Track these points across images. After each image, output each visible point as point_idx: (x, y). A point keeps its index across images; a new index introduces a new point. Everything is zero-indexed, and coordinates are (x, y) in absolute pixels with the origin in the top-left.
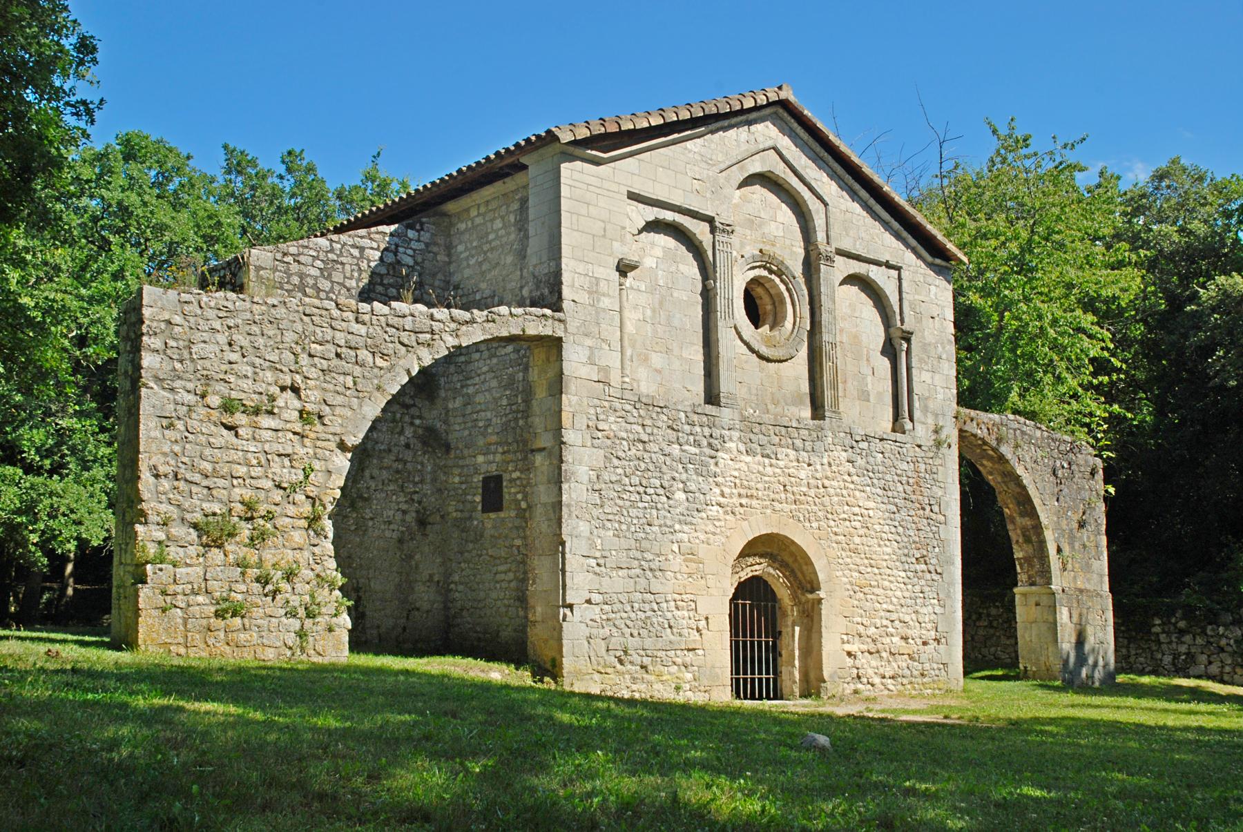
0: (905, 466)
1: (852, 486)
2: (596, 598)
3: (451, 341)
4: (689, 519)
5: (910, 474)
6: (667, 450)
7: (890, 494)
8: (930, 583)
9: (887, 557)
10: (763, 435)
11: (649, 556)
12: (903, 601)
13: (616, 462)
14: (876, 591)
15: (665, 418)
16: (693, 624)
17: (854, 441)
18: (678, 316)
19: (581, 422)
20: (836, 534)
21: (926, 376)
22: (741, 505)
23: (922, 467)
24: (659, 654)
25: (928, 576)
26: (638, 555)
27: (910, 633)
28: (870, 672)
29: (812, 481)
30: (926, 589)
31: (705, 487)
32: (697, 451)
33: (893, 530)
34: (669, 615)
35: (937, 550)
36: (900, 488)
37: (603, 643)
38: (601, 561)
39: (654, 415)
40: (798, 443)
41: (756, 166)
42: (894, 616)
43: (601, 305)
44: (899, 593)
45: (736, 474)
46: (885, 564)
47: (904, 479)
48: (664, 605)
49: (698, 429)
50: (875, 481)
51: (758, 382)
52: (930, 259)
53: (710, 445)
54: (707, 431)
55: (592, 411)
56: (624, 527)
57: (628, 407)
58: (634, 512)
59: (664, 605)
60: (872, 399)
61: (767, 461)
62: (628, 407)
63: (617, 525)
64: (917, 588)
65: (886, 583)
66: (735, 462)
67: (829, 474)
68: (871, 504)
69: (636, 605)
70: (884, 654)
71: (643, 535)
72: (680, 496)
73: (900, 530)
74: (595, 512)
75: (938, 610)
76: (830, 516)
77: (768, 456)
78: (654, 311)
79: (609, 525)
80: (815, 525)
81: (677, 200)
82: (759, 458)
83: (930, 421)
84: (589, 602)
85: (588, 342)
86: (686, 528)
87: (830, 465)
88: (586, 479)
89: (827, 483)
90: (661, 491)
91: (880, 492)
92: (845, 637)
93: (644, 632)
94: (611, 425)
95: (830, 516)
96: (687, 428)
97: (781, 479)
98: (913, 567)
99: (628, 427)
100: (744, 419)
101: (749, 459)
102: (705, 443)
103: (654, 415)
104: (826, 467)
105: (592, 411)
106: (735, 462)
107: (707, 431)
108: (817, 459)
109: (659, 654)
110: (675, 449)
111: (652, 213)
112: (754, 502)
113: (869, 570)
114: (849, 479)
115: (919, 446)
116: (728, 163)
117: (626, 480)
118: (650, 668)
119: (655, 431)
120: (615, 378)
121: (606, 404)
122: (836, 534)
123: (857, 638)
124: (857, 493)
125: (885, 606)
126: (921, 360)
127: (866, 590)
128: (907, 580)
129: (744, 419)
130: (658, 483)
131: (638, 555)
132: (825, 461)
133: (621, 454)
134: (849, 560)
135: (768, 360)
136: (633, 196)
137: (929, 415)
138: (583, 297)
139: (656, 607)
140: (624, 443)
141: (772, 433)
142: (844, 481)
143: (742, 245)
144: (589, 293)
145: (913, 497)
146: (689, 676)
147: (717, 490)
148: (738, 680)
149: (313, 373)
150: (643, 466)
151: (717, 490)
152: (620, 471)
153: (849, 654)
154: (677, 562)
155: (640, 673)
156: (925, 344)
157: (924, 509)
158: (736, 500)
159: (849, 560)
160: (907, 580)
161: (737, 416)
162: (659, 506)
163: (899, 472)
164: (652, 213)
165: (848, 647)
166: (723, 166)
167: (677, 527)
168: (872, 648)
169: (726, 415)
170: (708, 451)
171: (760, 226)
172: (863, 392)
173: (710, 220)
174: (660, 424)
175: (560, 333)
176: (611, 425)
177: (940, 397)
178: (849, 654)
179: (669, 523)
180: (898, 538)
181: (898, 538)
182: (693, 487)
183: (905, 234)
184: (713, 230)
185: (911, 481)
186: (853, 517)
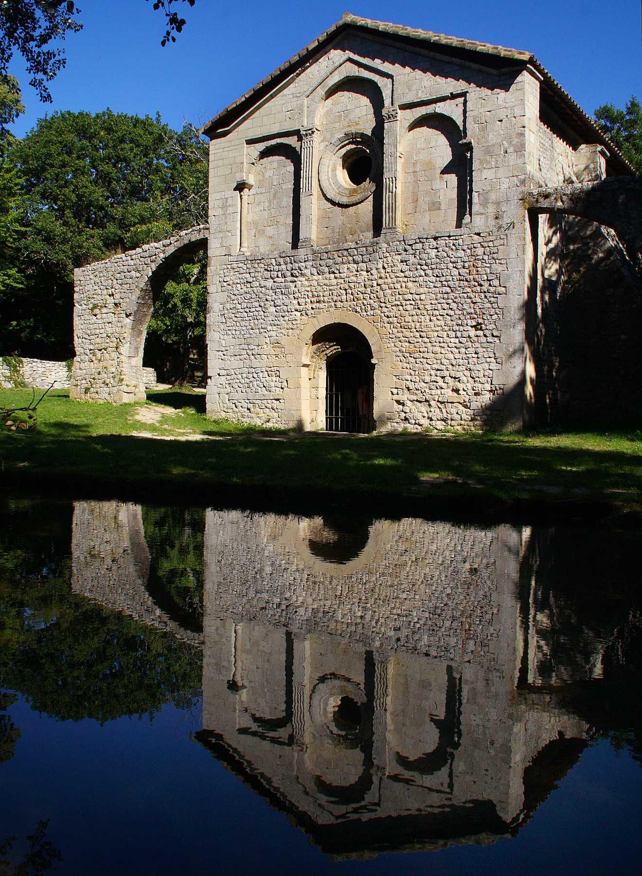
0: (461, 253)
1: (406, 279)
2: (223, 372)
3: (162, 255)
4: (276, 322)
5: (466, 259)
6: (263, 283)
7: (443, 279)
8: (485, 345)
9: (437, 329)
10: (328, 258)
11: (252, 347)
12: (454, 363)
13: (233, 297)
14: (426, 355)
15: (262, 266)
16: (279, 385)
17: (407, 245)
18: (285, 199)
19: (216, 279)
20: (388, 317)
21: (488, 174)
22: (312, 308)
23: (480, 251)
24: (257, 402)
25: (483, 339)
26: (246, 347)
27: (460, 386)
28: (419, 416)
29: (368, 283)
30: (480, 350)
31: (287, 301)
32: (283, 280)
33: (446, 306)
34: (263, 380)
35: (495, 317)
36: (455, 272)
37: (227, 396)
38: (225, 353)
39: (256, 266)
40: (358, 258)
41: (336, 78)
42: (446, 373)
43: (228, 212)
44: (451, 356)
45: (309, 289)
46: (436, 334)
47: (460, 265)
48: (261, 375)
49: (284, 267)
50: (429, 272)
51: (340, 222)
52: (495, 72)
53: (292, 275)
54: (289, 266)
55: (222, 272)
56: (238, 332)
57: (241, 265)
58: (243, 323)
59: (261, 375)
60: (443, 207)
61: (332, 276)
62: (241, 265)
63: (234, 332)
64: (472, 350)
65: (438, 349)
66: (311, 281)
67: (383, 275)
68: (422, 290)
69: (244, 375)
70: (433, 403)
71: (248, 336)
72: (273, 309)
73: (454, 306)
74: (222, 326)
75: (494, 366)
76: (383, 305)
77: (334, 273)
78: (270, 202)
79: (229, 332)
80: (371, 312)
81: (275, 130)
82: (327, 275)
83: (491, 210)
84: (219, 375)
85: (221, 235)
86: (274, 328)
87: (384, 268)
88: (217, 310)
89: (380, 281)
90: (260, 309)
91: (434, 279)
92: (395, 391)
93: (248, 390)
94: (232, 277)
95: (383, 305)
96: (276, 268)
97: (342, 286)
98: (465, 334)
99: (240, 276)
100: (314, 253)
101: (320, 277)
102: (289, 274)
103: (256, 266)
104: (382, 271)
105: (222, 272)
106: (311, 281)
107: (289, 266)
108: (372, 266)
109: (257, 402)
110: (270, 283)
111: (261, 146)
112: (321, 305)
113: (420, 340)
114: (402, 275)
115: (479, 234)
116: (311, 89)
117: (239, 306)
118: (252, 409)
119: (256, 274)
120: (235, 251)
121: (229, 267)
122: (388, 317)
123: (406, 391)
124: (410, 284)
125: (435, 366)
126: (481, 163)
127: (416, 355)
128: (459, 345)
129: (314, 253)
130: (257, 304)
131: (246, 347)
132: (380, 266)
133: (236, 292)
134: (400, 335)
135: (346, 206)
136: (250, 142)
137: (489, 205)
138: (218, 212)
139: (255, 376)
140: (238, 286)
141: (336, 256)
142: (396, 277)
143: (332, 135)
144: (222, 208)
145: (468, 277)
146: (276, 415)
147: (295, 302)
148: (331, 419)
149: (117, 286)
150: (248, 296)
151: (295, 302)
152: (236, 302)
153: (398, 402)
154: (268, 349)
155: (247, 413)
156: (488, 147)
157: (481, 285)
158: (309, 306)
159: (400, 335)
160: (459, 345)
161: (309, 252)
162: (259, 317)
163: (452, 260)
164: (261, 146)
165: (396, 397)
166: (307, 93)
167: (269, 328)
168: (420, 397)
169: (302, 253)
170: (289, 279)
171: (346, 117)
172: (434, 203)
173: (297, 133)
174: (259, 269)
175: (207, 236)
176: (232, 277)
177: (504, 186)
178: (398, 402)
179: (263, 326)
180: (452, 313)
181: (452, 313)
182: (278, 302)
183: (467, 64)
184: (300, 139)
185: (466, 265)
186: (404, 303)
